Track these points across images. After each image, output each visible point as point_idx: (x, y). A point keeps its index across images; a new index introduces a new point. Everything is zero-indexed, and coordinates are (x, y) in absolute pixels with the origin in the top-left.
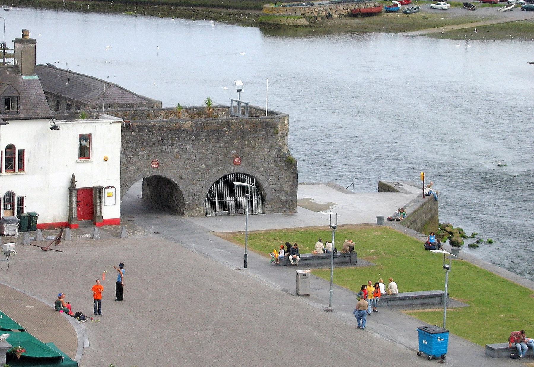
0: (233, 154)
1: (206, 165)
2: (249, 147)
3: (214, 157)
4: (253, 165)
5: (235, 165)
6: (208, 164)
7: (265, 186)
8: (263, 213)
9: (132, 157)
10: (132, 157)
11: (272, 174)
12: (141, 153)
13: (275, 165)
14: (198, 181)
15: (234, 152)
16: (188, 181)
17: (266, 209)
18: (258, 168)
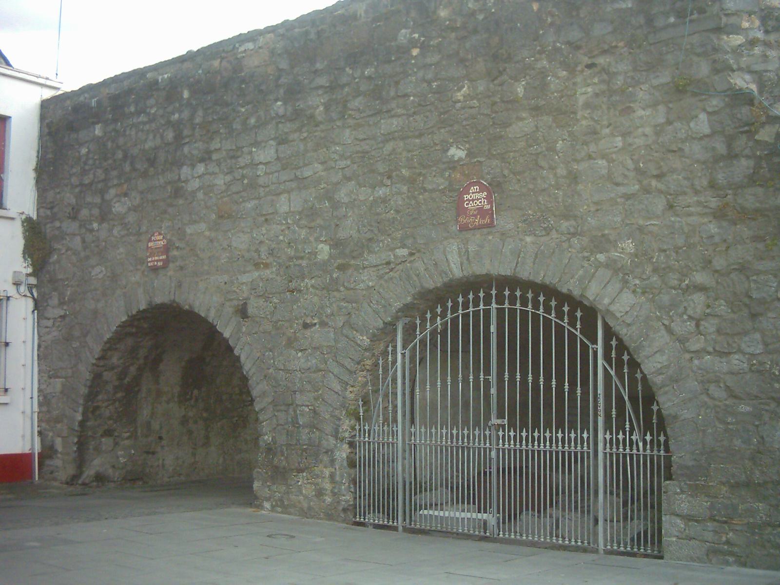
0: (453, 165)
1: (336, 244)
2: (536, 110)
3: (364, 194)
4: (565, 225)
5: (464, 228)
6: (342, 234)
7: (655, 361)
8: (650, 544)
9: (95, 225)
10: (95, 225)
11: (700, 278)
12: (118, 208)
13: (719, 215)
14: (306, 326)
15: (457, 153)
16: (268, 327)
17: (672, 526)
18: (601, 243)
